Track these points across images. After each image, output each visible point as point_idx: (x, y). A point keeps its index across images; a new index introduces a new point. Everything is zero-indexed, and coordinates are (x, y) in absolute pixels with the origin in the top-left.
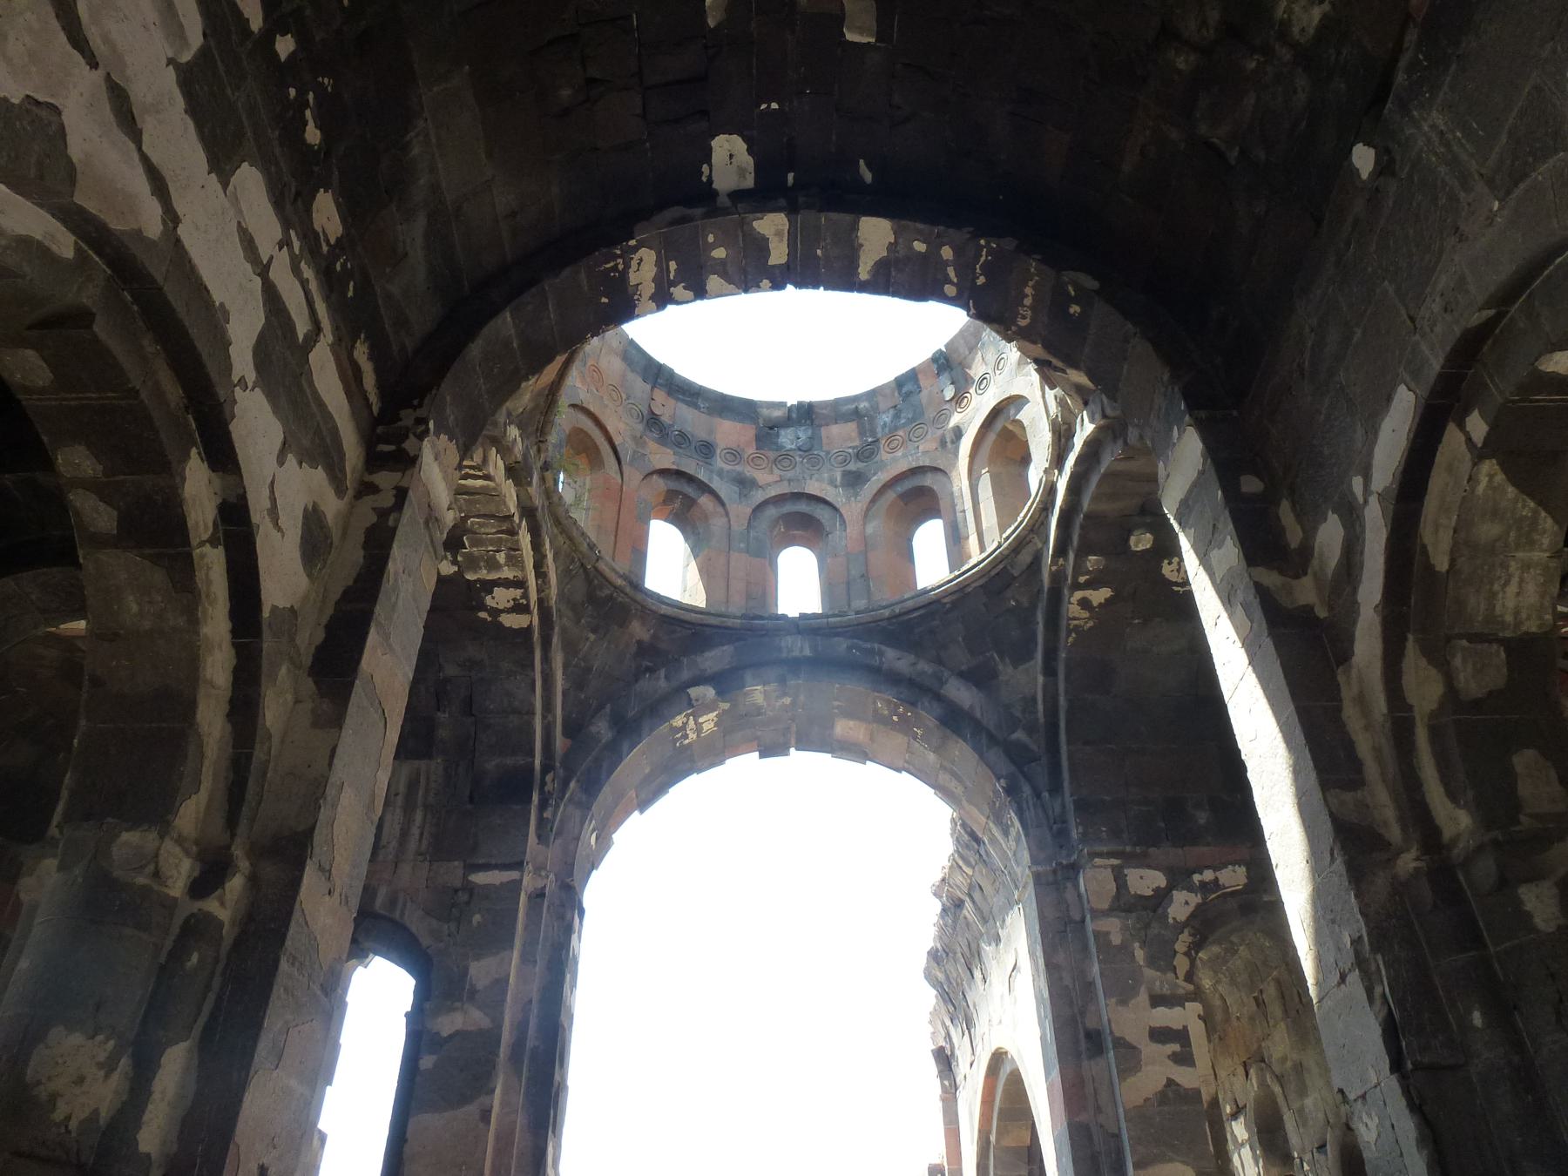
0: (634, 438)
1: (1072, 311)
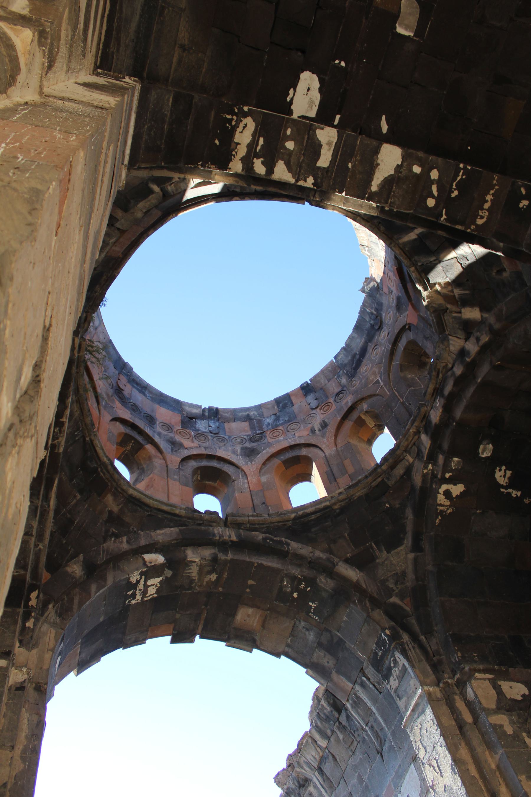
1: (521, 205)
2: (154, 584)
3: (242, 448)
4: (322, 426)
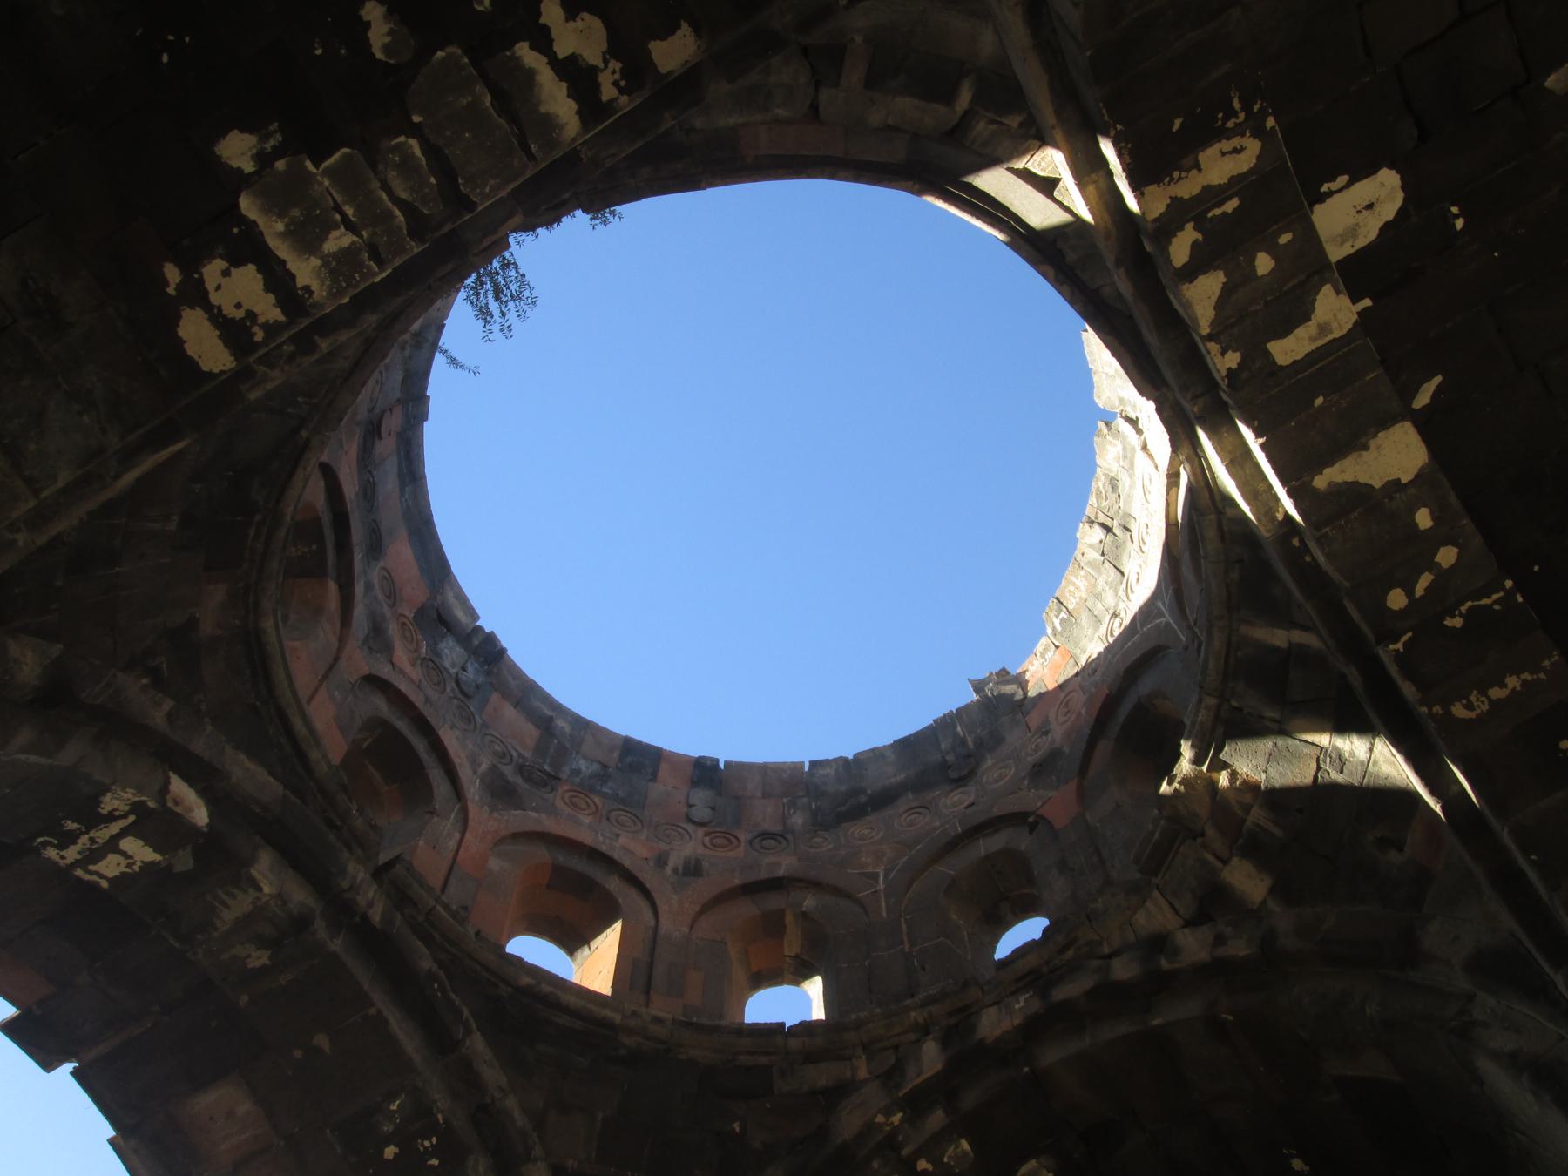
2: (131, 857)
3: (493, 769)
4: (686, 866)
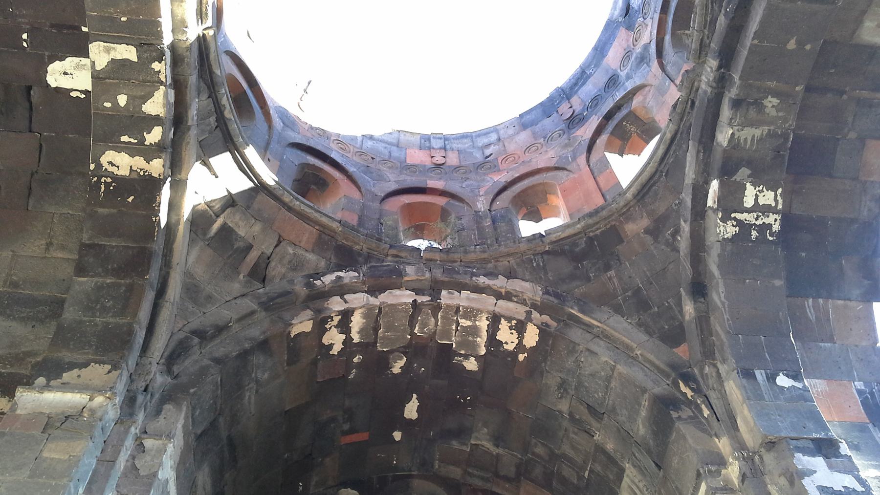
0: (566, 146)
